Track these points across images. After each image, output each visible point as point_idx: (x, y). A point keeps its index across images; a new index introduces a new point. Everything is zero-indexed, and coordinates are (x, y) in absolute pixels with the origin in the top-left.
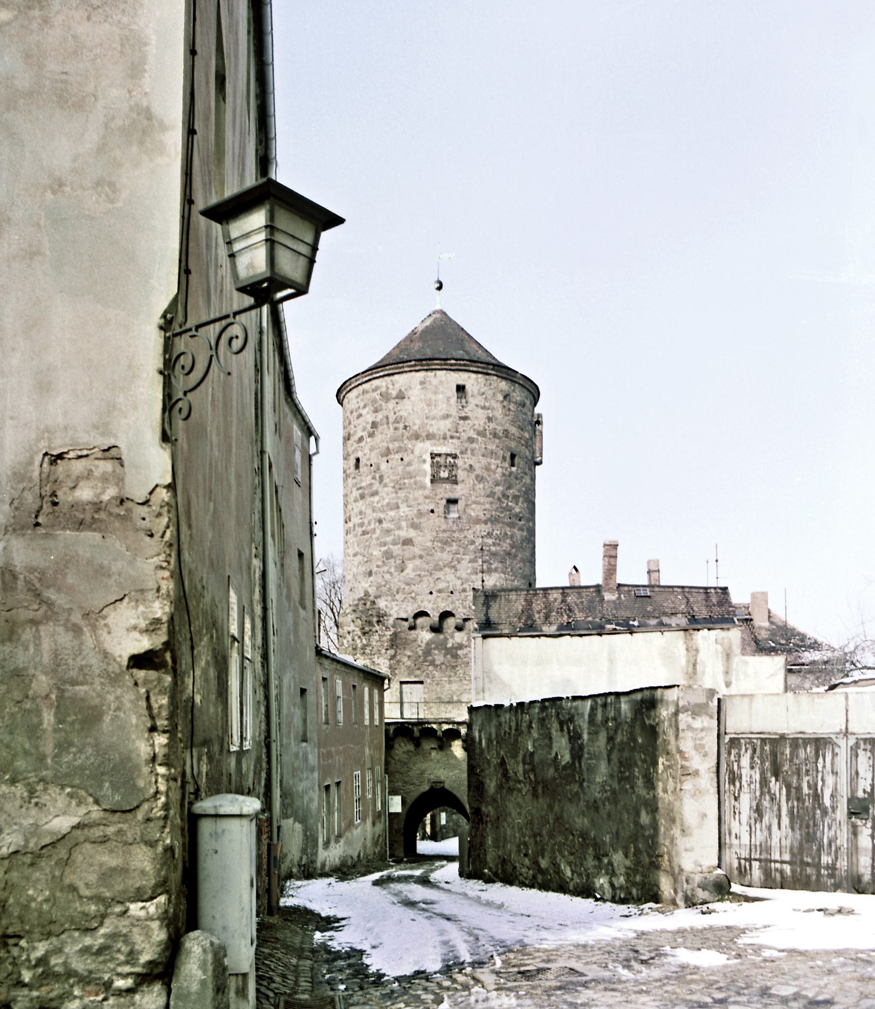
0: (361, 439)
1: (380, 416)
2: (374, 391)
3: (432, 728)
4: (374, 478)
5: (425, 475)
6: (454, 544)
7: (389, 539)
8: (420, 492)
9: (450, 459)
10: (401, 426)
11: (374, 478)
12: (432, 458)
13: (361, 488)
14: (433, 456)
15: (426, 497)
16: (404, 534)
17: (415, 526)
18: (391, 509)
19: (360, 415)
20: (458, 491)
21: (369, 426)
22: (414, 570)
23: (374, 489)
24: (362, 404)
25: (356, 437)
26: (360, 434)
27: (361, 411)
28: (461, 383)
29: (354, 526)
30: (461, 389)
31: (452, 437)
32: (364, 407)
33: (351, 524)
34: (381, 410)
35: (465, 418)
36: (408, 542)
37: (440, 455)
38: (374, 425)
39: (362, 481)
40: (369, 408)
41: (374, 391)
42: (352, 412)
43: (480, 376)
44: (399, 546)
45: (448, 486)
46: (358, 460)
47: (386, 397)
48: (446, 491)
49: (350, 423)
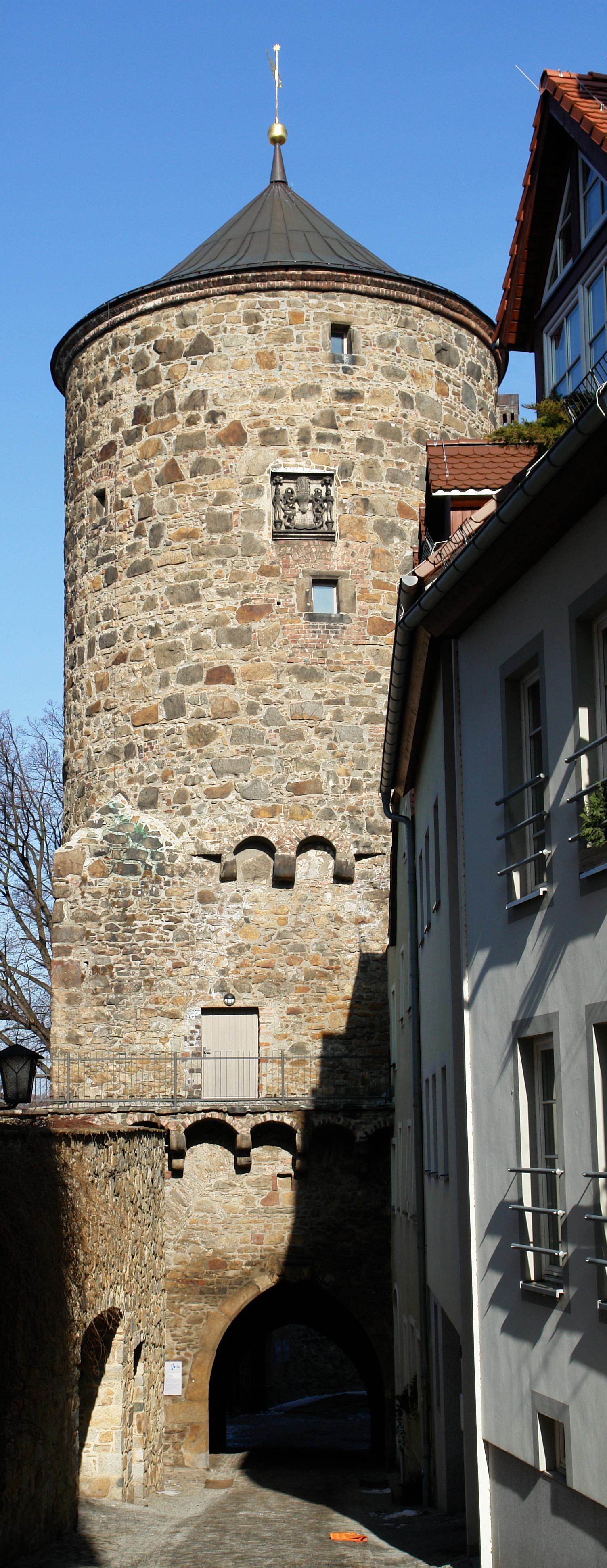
0: (109, 449)
1: (152, 395)
2: (139, 340)
3: (281, 1125)
4: (139, 533)
5: (260, 523)
6: (330, 678)
7: (173, 670)
8: (250, 561)
9: (315, 486)
10: (203, 413)
11: (139, 533)
12: (277, 484)
13: (108, 558)
14: (277, 478)
15: (266, 571)
16: (210, 658)
17: (237, 638)
18: (181, 602)
19: (106, 398)
20: (335, 558)
21: (128, 419)
22: (234, 740)
23: (140, 557)
24: (111, 372)
25: (98, 447)
26: (106, 436)
27: (109, 388)
28: (341, 318)
29: (91, 644)
30: (340, 330)
31: (321, 438)
32: (118, 376)
33: (82, 642)
34: (157, 380)
35: (350, 396)
36: (221, 675)
37: (293, 476)
38: (141, 415)
39: (111, 541)
40: (129, 382)
41: (139, 340)
42: (86, 395)
43: (381, 304)
44: (200, 684)
45: (314, 546)
46: (101, 495)
47: (168, 351)
48: (309, 558)
49: (83, 417)
